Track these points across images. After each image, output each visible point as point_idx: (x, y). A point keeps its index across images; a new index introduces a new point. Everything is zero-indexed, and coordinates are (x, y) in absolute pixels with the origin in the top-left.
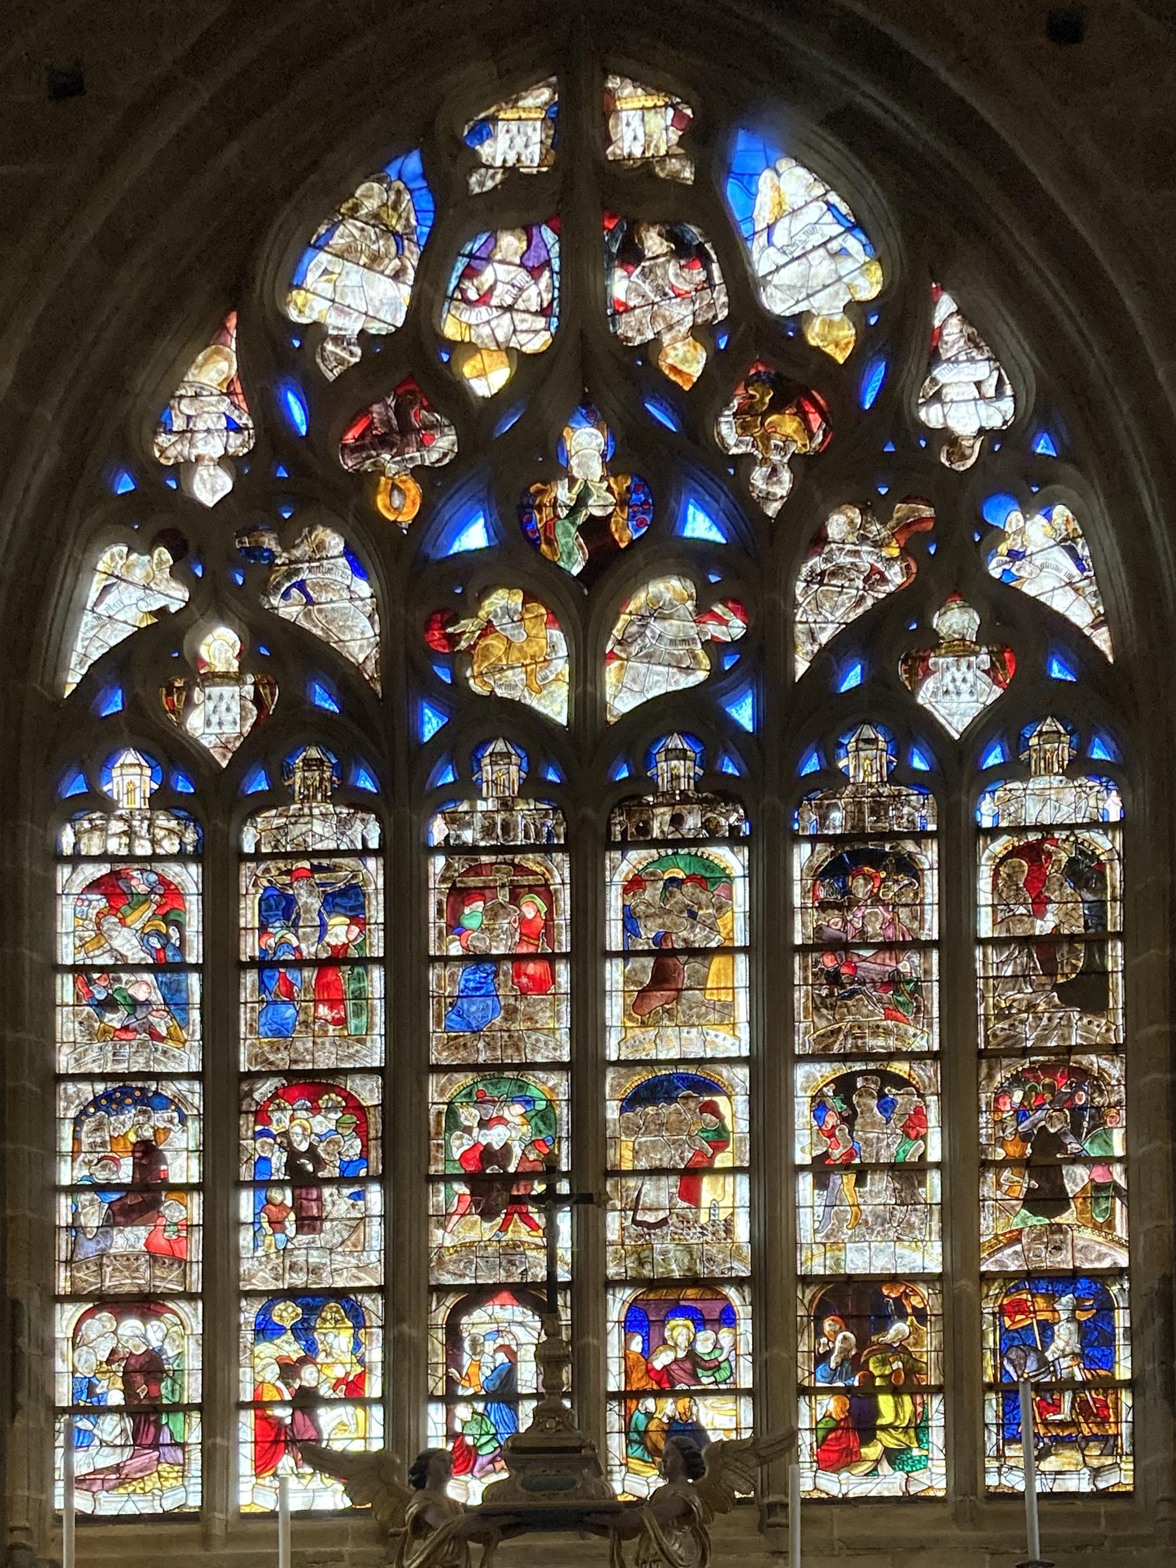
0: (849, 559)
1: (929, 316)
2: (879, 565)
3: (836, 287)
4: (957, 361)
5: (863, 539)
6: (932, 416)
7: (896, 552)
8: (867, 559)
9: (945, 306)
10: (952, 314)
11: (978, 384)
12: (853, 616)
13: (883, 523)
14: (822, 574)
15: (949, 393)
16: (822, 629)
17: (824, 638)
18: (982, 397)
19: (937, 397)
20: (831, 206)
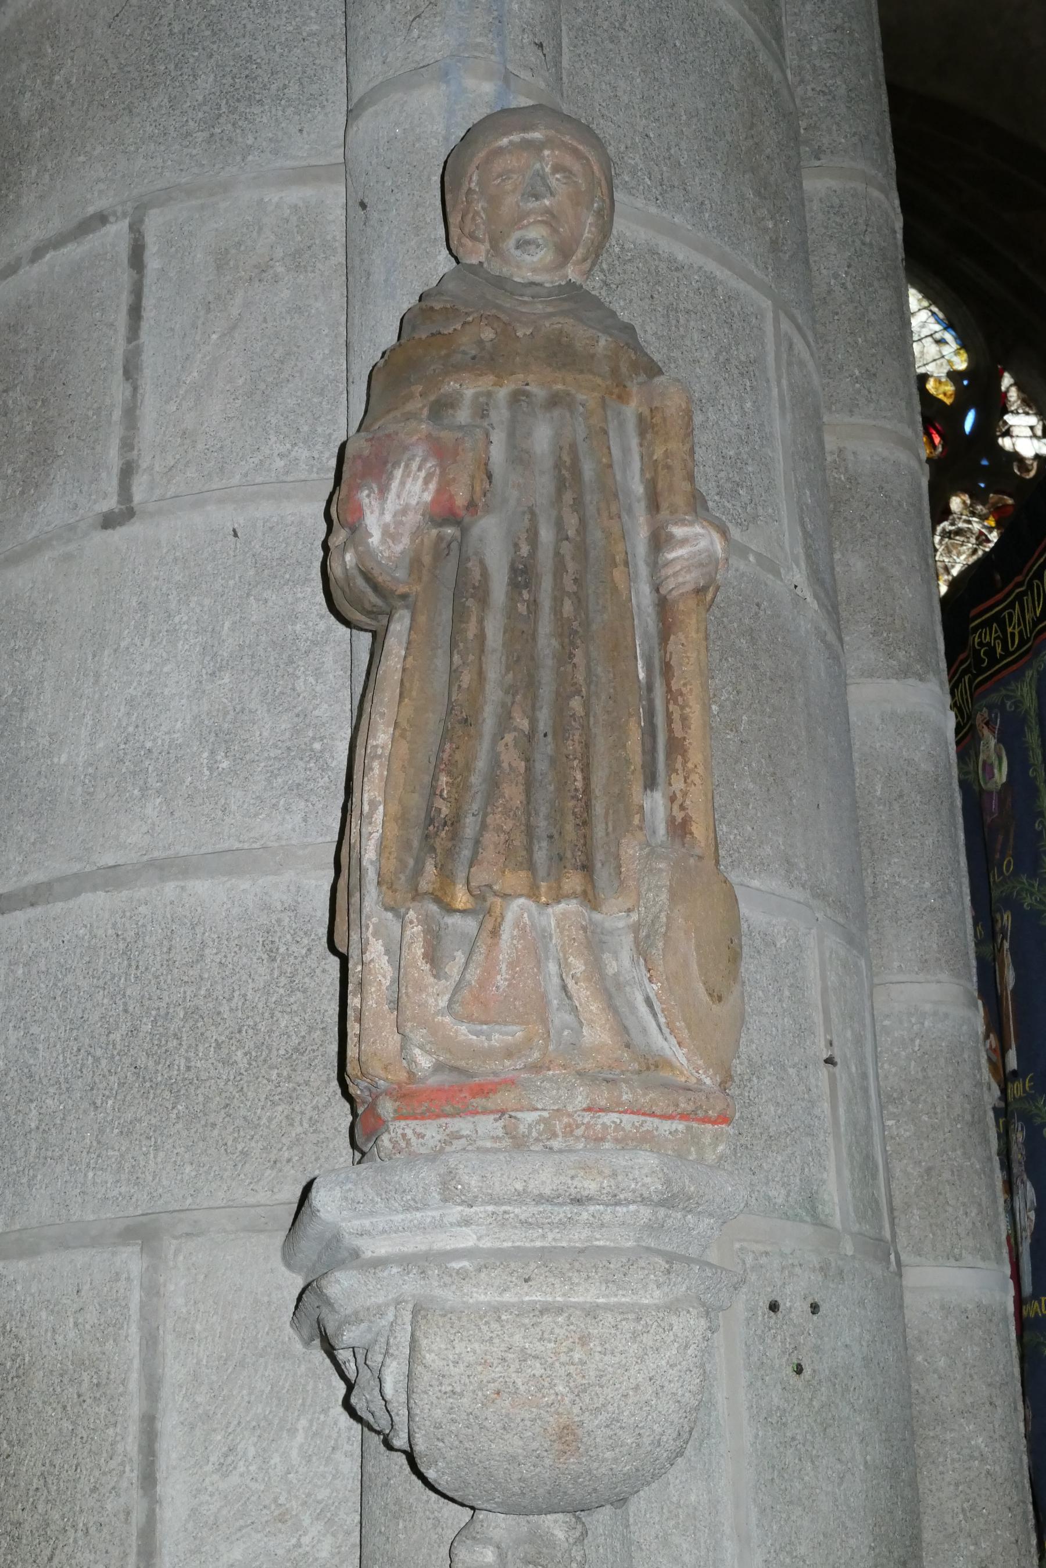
0: (966, 525)
1: (1000, 386)
2: (984, 531)
3: (942, 360)
4: (1018, 413)
5: (973, 514)
6: (1006, 443)
7: (993, 524)
8: (976, 526)
9: (1007, 380)
10: (1011, 385)
11: (1032, 428)
12: (971, 560)
13: (984, 505)
14: (950, 532)
15: (1015, 431)
16: (953, 567)
17: (955, 572)
18: (1035, 436)
19: (1008, 433)
20: (933, 314)
